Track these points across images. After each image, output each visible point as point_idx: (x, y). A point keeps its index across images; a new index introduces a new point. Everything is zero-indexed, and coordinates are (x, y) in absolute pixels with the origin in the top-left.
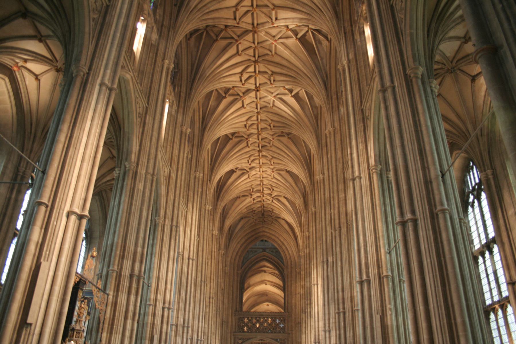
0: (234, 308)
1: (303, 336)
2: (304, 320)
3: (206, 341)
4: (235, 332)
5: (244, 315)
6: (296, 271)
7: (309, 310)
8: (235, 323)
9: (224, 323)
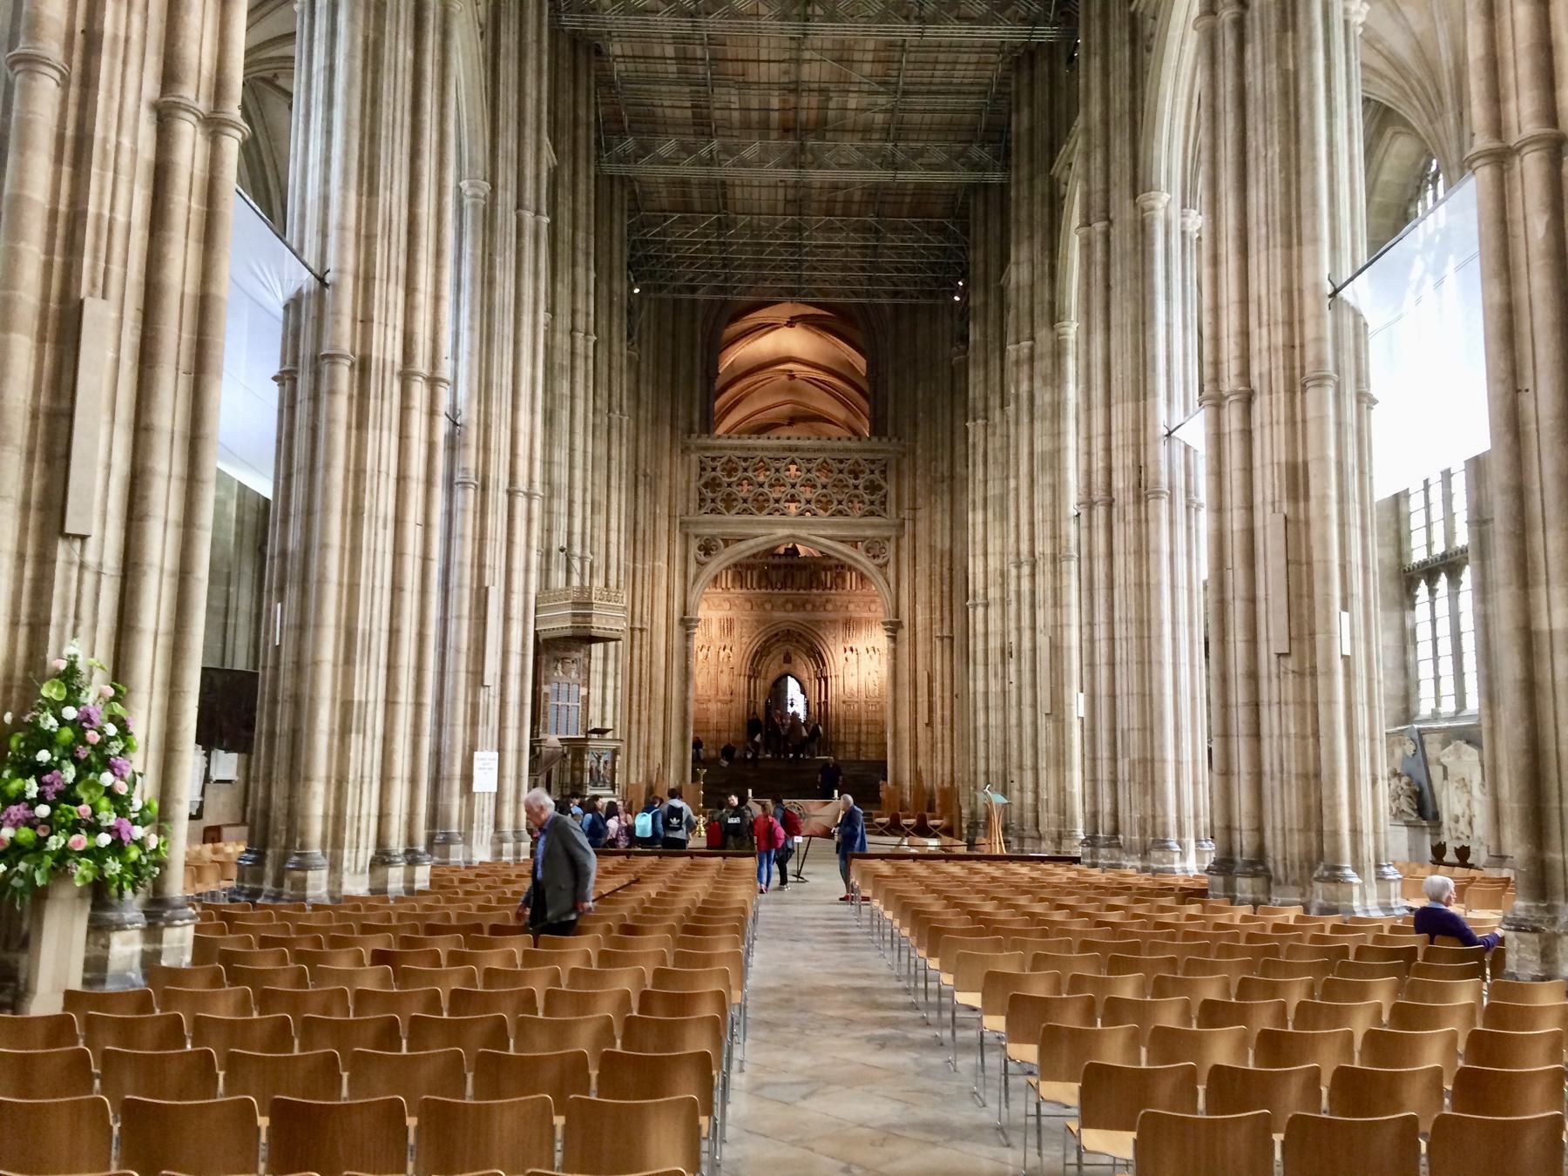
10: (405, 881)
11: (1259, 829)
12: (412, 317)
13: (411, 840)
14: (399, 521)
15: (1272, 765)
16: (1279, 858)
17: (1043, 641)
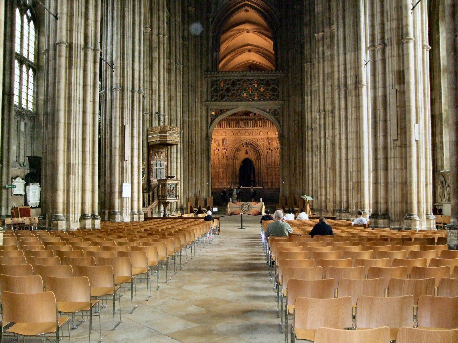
0: (205, 68)
1: (308, 98)
2: (309, 74)
3: (157, 103)
4: (207, 101)
5: (218, 77)
6: (293, 8)
7: (321, 49)
8: (207, 89)
9: (190, 87)
10: (92, 225)
11: (387, 203)
12: (87, 28)
13: (93, 211)
14: (84, 101)
15: (391, 180)
16: (393, 212)
17: (328, 142)
